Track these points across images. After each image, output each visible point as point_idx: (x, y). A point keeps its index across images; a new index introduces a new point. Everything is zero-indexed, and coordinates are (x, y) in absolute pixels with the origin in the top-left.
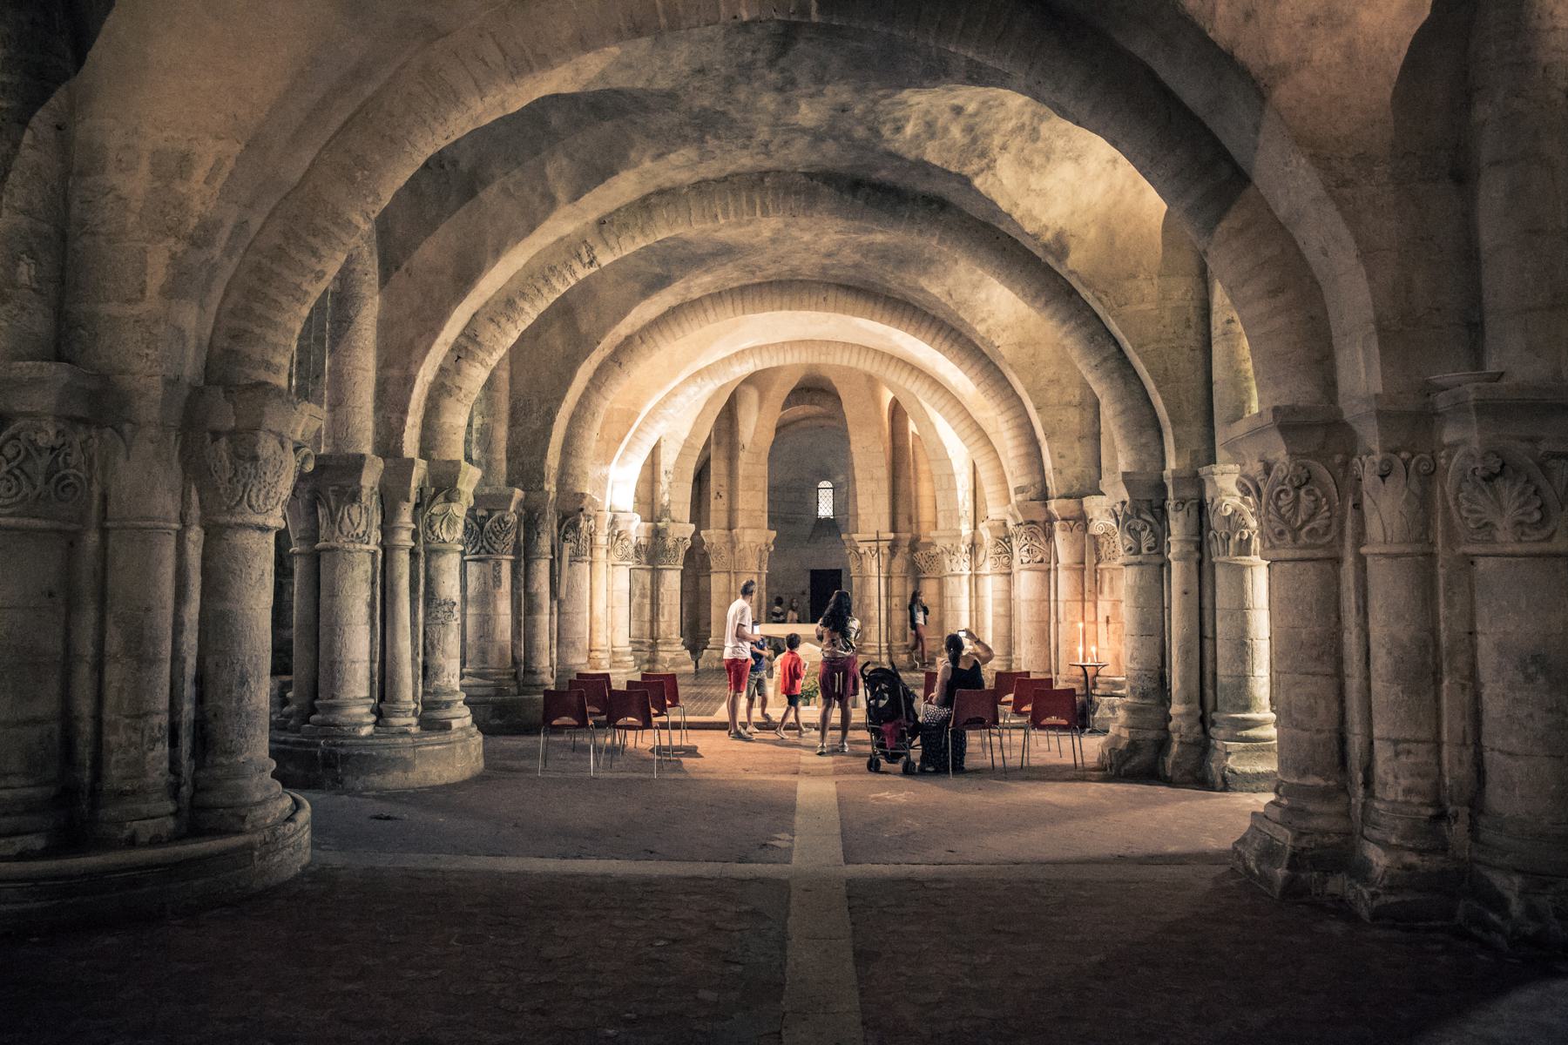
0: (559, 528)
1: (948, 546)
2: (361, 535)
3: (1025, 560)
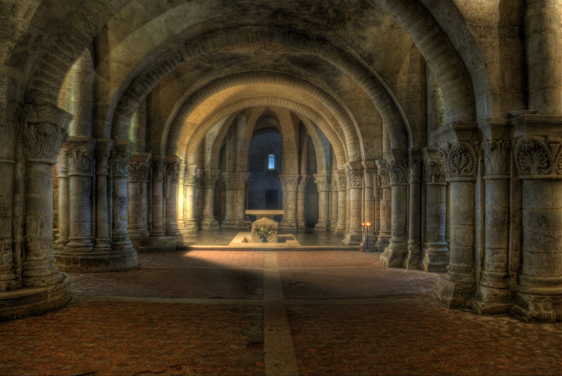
0: (167, 169)
1: (321, 180)
2: (87, 170)
3: (352, 184)
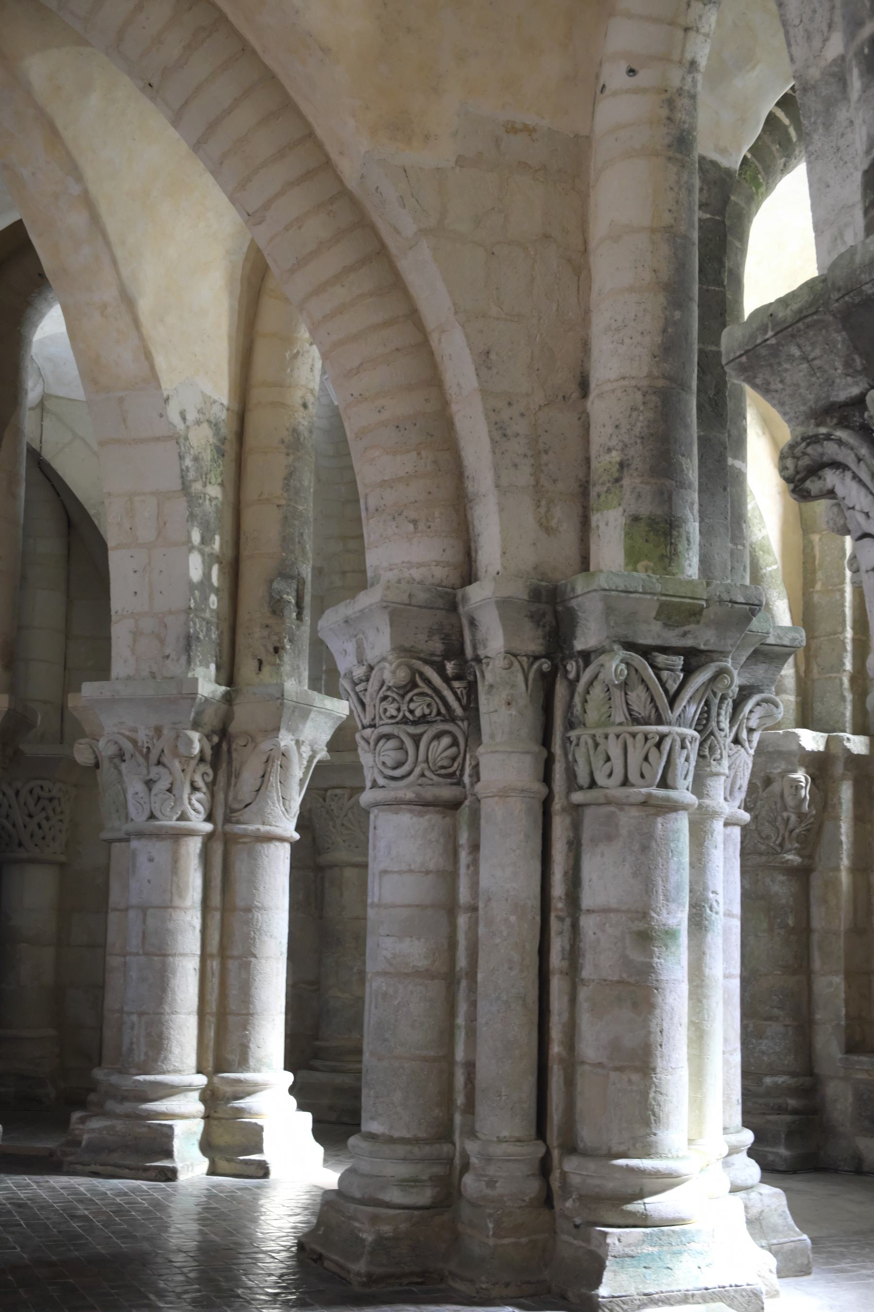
1: (142, 736)
